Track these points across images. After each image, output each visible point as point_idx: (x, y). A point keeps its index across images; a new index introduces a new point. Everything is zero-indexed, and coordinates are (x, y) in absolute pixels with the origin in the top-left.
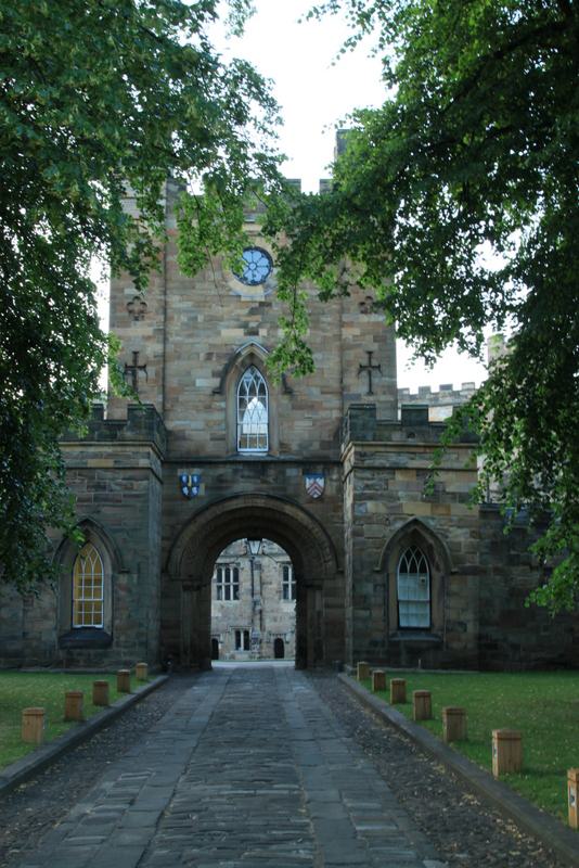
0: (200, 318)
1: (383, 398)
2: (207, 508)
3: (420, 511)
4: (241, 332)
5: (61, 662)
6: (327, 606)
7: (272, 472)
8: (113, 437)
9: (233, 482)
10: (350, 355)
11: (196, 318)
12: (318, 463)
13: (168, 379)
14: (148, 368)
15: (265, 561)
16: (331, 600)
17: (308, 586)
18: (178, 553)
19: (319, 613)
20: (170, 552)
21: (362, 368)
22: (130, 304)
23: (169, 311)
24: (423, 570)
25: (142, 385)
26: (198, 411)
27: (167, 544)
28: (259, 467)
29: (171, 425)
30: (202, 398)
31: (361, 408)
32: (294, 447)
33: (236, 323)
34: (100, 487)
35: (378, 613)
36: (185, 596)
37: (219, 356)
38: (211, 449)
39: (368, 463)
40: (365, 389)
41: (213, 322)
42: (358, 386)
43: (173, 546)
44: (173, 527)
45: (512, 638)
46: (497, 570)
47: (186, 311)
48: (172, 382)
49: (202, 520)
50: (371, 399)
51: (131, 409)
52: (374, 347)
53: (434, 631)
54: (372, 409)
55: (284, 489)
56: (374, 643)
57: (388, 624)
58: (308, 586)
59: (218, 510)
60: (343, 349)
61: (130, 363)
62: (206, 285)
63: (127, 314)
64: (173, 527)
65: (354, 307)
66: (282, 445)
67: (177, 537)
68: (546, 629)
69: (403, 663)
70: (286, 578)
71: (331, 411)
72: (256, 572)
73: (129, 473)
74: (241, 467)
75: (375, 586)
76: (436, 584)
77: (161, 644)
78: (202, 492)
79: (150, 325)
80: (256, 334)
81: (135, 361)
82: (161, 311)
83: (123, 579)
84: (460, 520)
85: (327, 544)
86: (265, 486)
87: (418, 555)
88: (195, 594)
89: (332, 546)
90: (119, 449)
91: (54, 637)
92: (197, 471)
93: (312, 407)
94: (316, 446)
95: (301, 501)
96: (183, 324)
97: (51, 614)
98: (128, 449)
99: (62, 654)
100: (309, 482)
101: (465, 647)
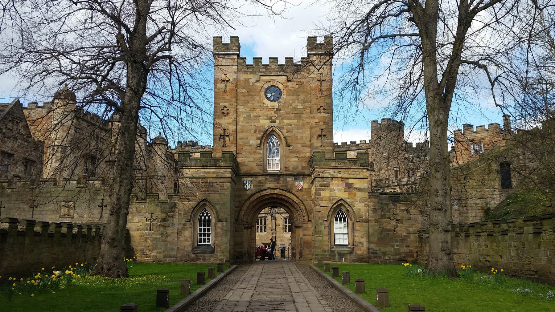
0: (252, 115)
1: (327, 148)
2: (254, 194)
3: (343, 195)
4: (268, 121)
5: (193, 260)
6: (304, 235)
7: (281, 179)
8: (216, 165)
9: (265, 183)
10: (314, 130)
11: (250, 115)
12: (301, 175)
13: (238, 140)
14: (230, 136)
15: (277, 215)
16: (306, 233)
17: (296, 227)
18: (242, 213)
19: (301, 238)
20: (239, 212)
21: (319, 136)
22: (222, 109)
23: (238, 113)
24: (345, 220)
25: (227, 143)
26: (251, 154)
27: (238, 209)
28: (276, 177)
29: (239, 160)
30: (252, 148)
31: (318, 152)
32: (291, 169)
33: (266, 117)
34: (210, 186)
35: (326, 238)
36: (245, 230)
37: (260, 131)
38: (256, 170)
39: (321, 176)
40: (320, 144)
41: (257, 117)
42: (317, 144)
43: (240, 210)
44: (240, 202)
45: (383, 249)
46: (376, 221)
47: (246, 113)
48: (240, 142)
49: (252, 199)
50: (323, 148)
51: (223, 153)
52: (324, 127)
53: (350, 246)
54: (323, 153)
55: (287, 186)
56: (325, 251)
57: (330, 243)
58: (296, 227)
59: (258, 195)
60: (311, 128)
61: (223, 134)
62: (254, 102)
63: (220, 113)
64: (240, 202)
65: (315, 111)
66: (285, 168)
67: (241, 208)
68: (397, 246)
69: (337, 260)
70: (286, 223)
71: (307, 153)
72: (273, 220)
73: (222, 180)
74: (268, 177)
75: (325, 227)
76: (350, 226)
77: (235, 251)
78: (252, 188)
79: (231, 118)
80: (275, 122)
81: (224, 133)
82: (235, 112)
83: (219, 224)
84: (361, 199)
85: (304, 209)
86: (279, 185)
87: (343, 214)
88: (249, 230)
89: (306, 210)
90: (218, 170)
91: (190, 249)
92: (250, 179)
93: (298, 152)
94: (300, 168)
95: (294, 191)
96: (244, 118)
97: (189, 239)
98: (222, 170)
99: (193, 256)
100: (297, 183)
101: (363, 253)
